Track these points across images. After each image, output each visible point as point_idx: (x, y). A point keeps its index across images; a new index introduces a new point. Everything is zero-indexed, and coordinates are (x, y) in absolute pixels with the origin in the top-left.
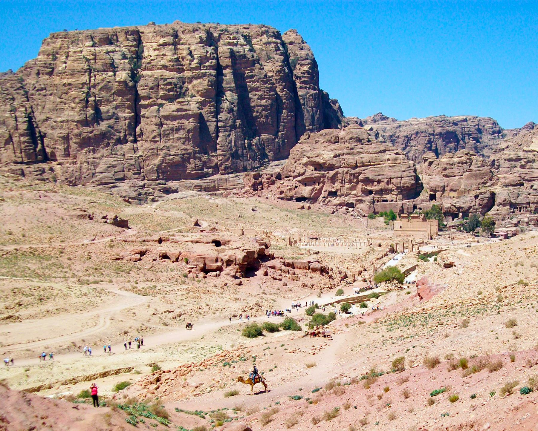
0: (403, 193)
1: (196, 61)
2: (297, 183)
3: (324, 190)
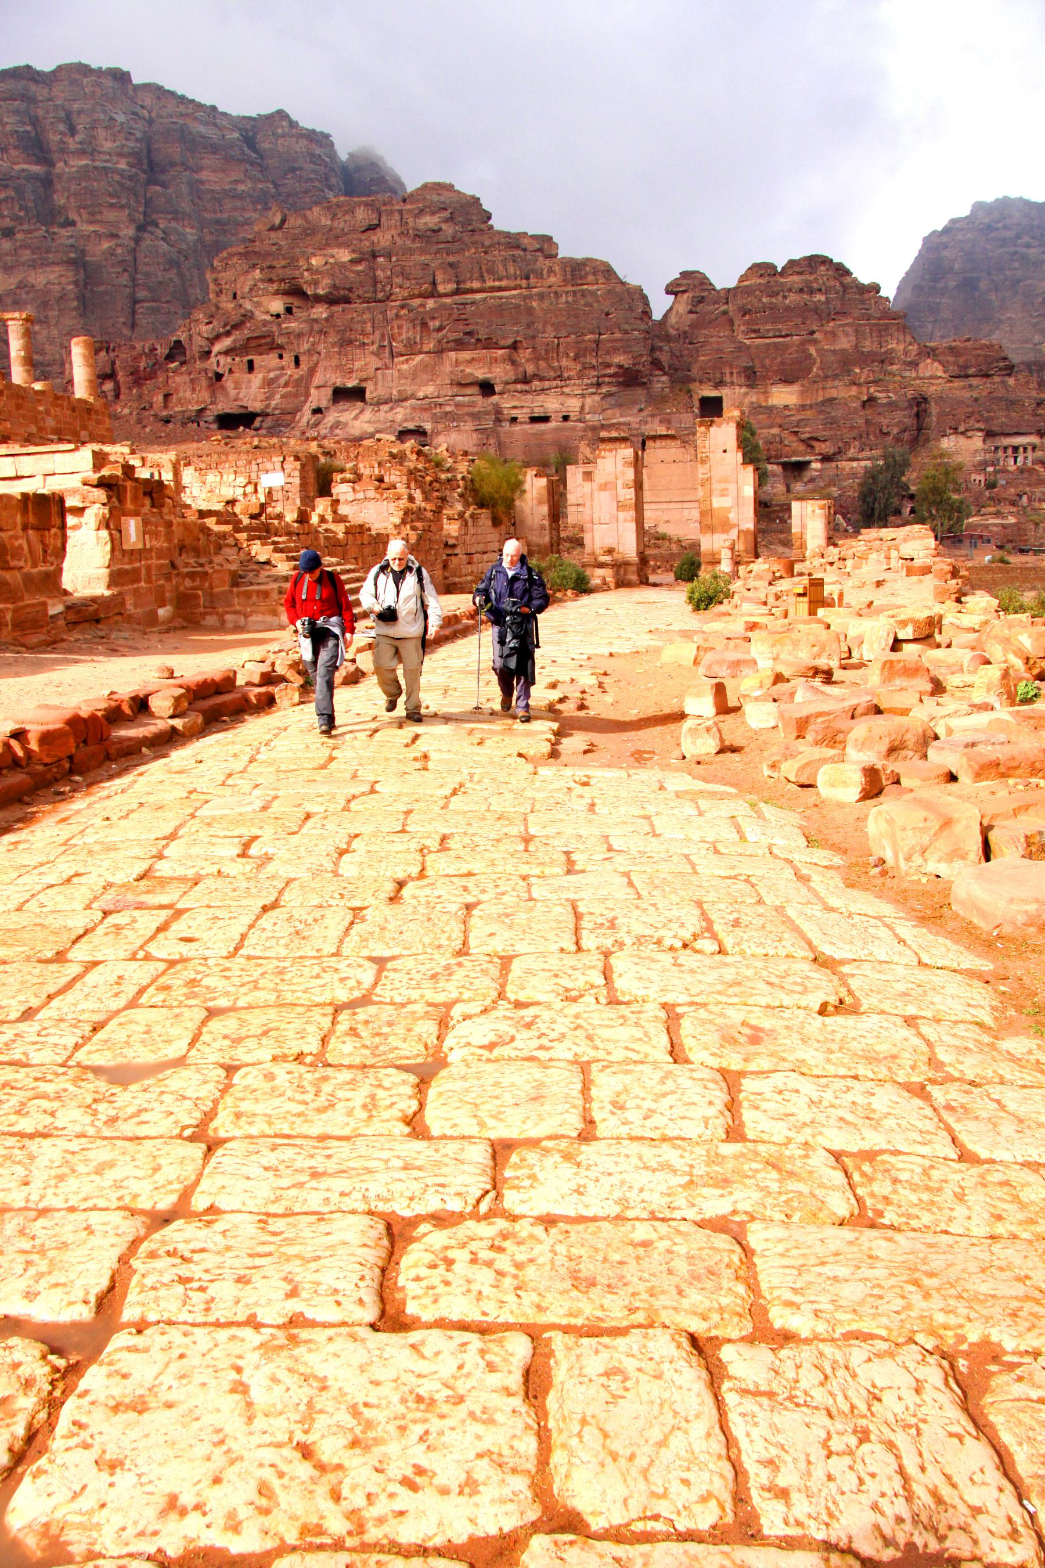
0: (604, 390)
1: (78, 138)
2: (222, 360)
3: (318, 380)
